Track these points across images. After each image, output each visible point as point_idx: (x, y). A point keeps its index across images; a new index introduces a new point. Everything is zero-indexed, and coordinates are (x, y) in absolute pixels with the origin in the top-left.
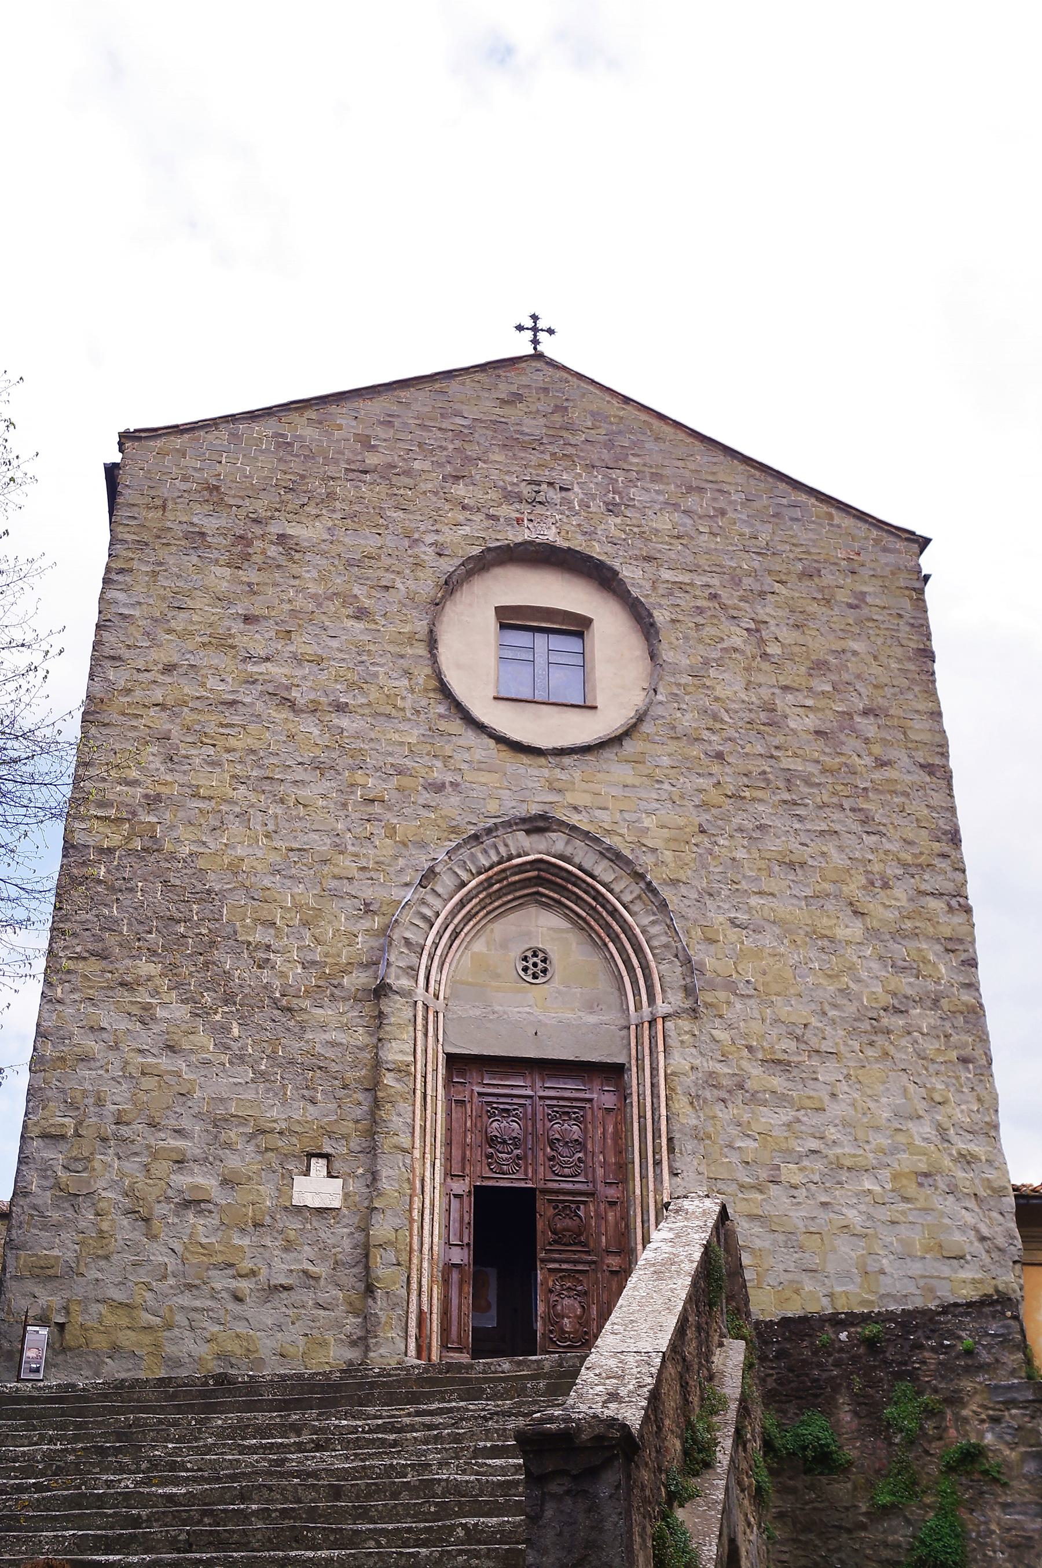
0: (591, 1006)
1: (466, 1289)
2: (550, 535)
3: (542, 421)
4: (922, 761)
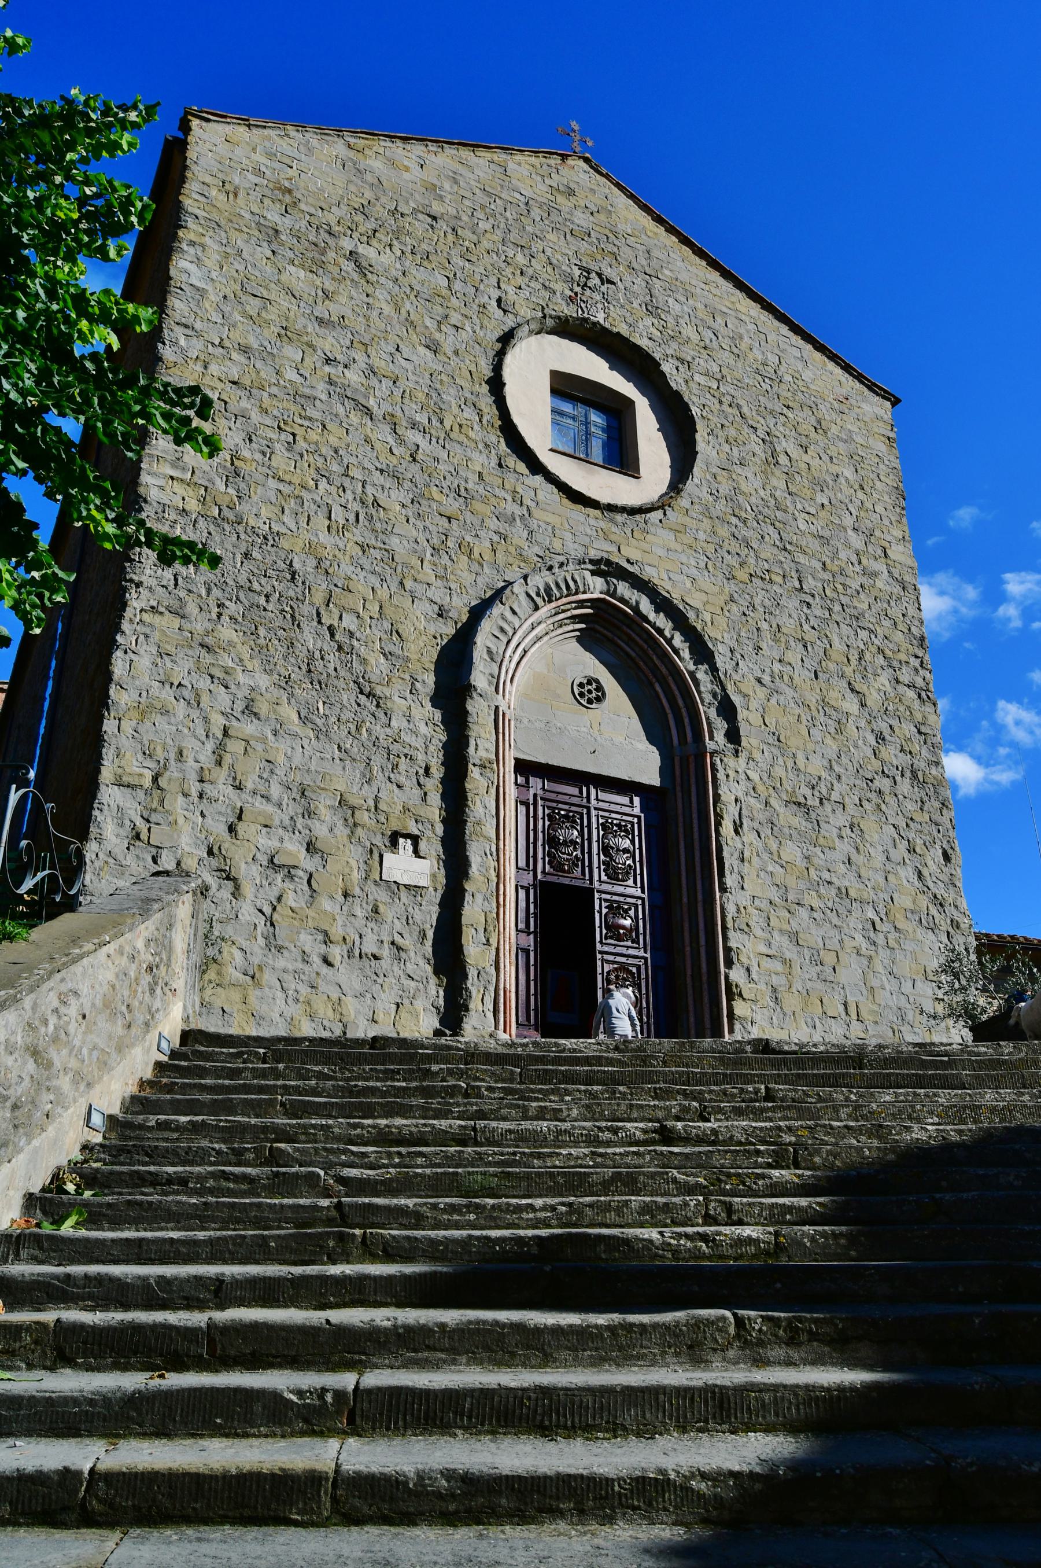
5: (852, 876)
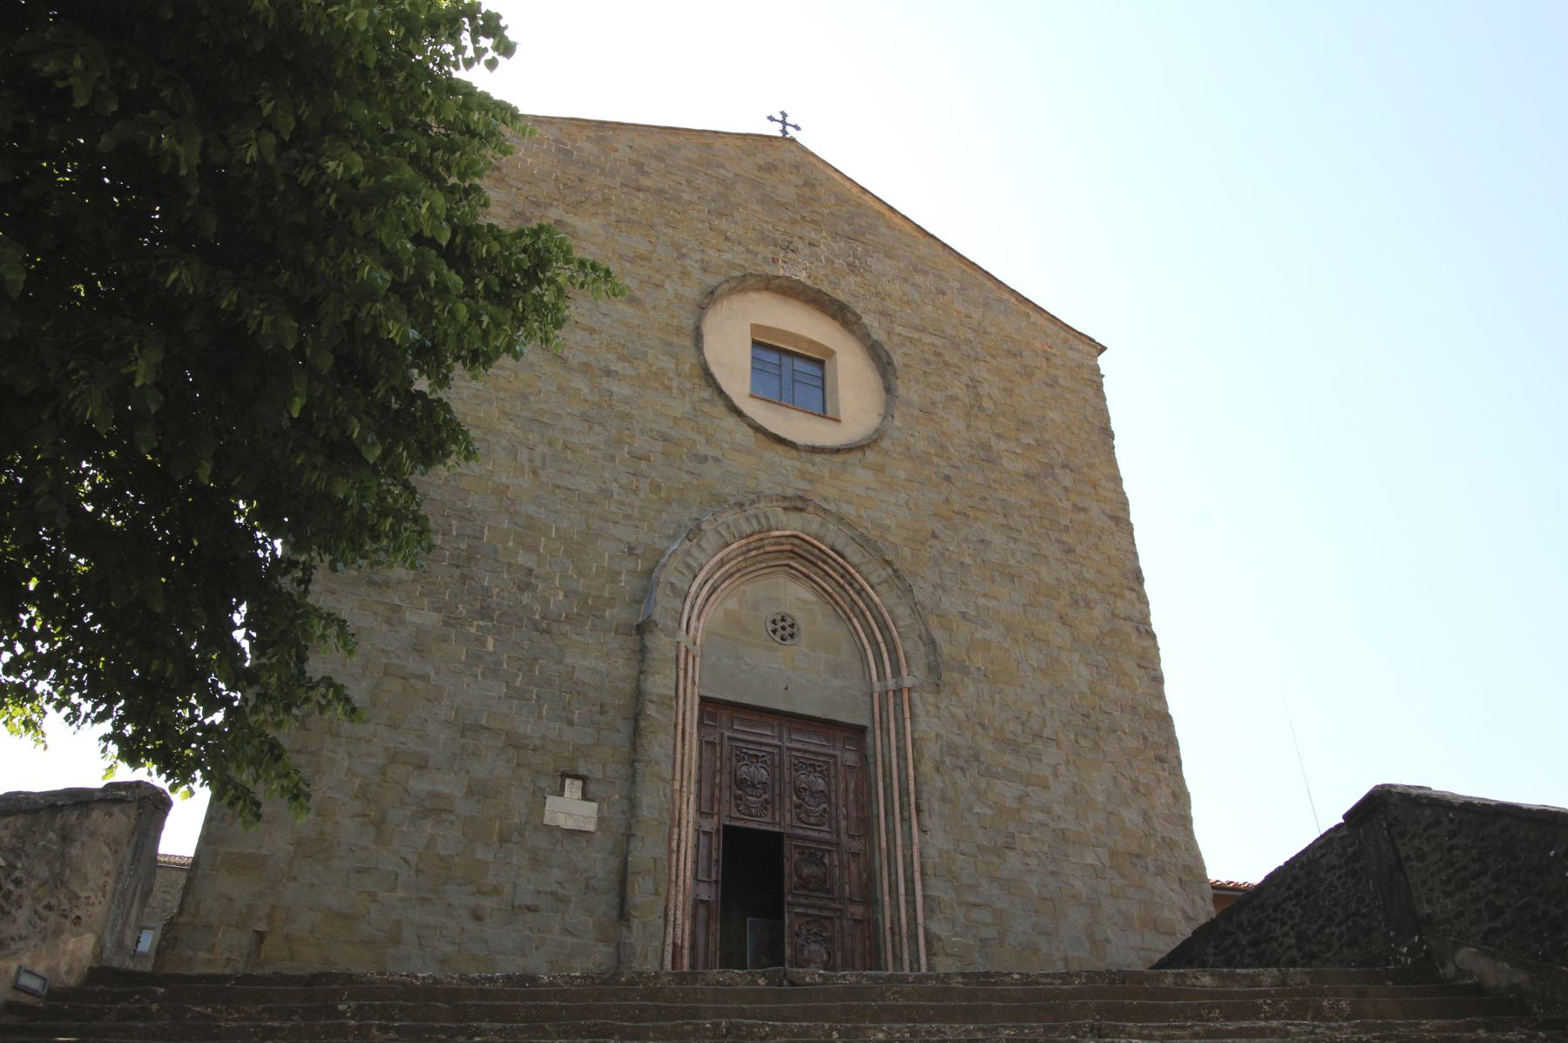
1: (713, 927)
2: (803, 276)
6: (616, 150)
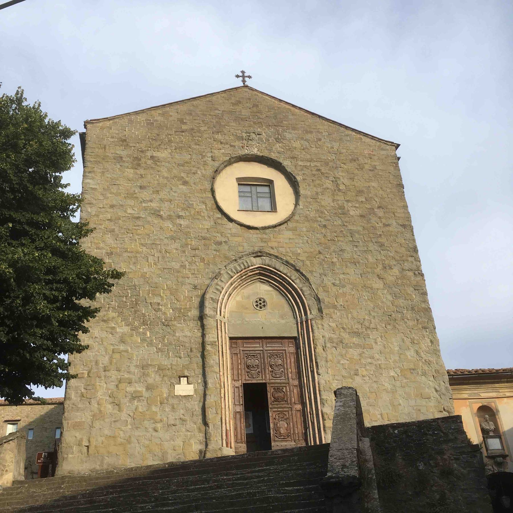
0: (282, 317)
1: (242, 420)
3: (250, 110)
4: (401, 224)
5: (383, 358)
6: (171, 116)
